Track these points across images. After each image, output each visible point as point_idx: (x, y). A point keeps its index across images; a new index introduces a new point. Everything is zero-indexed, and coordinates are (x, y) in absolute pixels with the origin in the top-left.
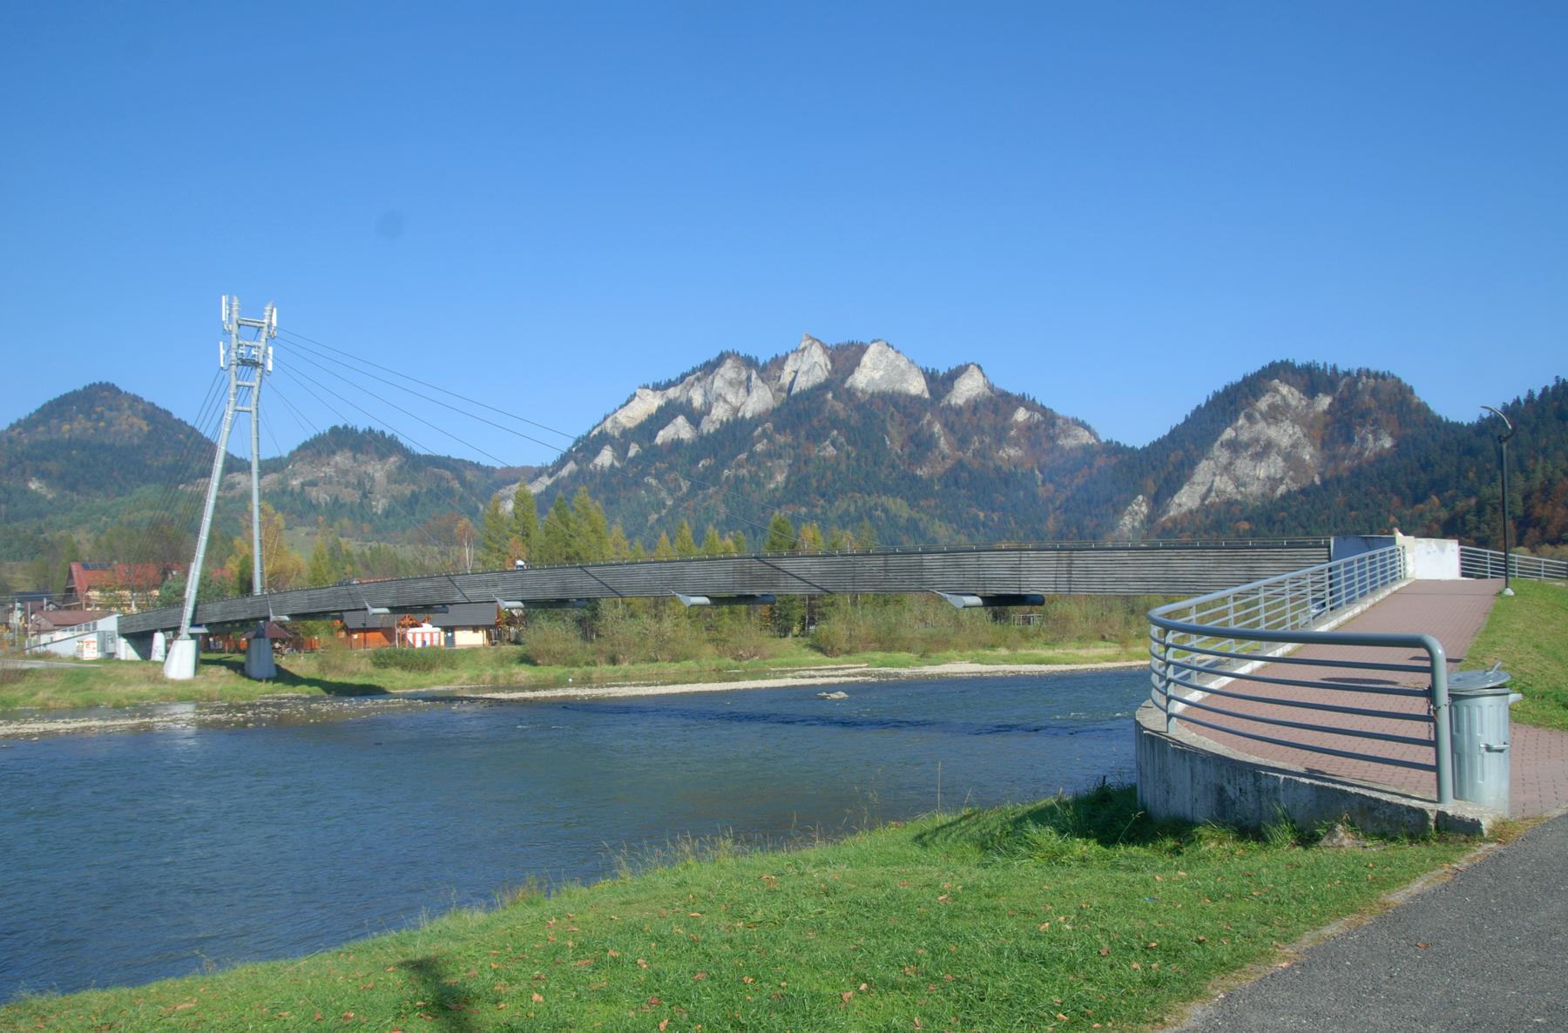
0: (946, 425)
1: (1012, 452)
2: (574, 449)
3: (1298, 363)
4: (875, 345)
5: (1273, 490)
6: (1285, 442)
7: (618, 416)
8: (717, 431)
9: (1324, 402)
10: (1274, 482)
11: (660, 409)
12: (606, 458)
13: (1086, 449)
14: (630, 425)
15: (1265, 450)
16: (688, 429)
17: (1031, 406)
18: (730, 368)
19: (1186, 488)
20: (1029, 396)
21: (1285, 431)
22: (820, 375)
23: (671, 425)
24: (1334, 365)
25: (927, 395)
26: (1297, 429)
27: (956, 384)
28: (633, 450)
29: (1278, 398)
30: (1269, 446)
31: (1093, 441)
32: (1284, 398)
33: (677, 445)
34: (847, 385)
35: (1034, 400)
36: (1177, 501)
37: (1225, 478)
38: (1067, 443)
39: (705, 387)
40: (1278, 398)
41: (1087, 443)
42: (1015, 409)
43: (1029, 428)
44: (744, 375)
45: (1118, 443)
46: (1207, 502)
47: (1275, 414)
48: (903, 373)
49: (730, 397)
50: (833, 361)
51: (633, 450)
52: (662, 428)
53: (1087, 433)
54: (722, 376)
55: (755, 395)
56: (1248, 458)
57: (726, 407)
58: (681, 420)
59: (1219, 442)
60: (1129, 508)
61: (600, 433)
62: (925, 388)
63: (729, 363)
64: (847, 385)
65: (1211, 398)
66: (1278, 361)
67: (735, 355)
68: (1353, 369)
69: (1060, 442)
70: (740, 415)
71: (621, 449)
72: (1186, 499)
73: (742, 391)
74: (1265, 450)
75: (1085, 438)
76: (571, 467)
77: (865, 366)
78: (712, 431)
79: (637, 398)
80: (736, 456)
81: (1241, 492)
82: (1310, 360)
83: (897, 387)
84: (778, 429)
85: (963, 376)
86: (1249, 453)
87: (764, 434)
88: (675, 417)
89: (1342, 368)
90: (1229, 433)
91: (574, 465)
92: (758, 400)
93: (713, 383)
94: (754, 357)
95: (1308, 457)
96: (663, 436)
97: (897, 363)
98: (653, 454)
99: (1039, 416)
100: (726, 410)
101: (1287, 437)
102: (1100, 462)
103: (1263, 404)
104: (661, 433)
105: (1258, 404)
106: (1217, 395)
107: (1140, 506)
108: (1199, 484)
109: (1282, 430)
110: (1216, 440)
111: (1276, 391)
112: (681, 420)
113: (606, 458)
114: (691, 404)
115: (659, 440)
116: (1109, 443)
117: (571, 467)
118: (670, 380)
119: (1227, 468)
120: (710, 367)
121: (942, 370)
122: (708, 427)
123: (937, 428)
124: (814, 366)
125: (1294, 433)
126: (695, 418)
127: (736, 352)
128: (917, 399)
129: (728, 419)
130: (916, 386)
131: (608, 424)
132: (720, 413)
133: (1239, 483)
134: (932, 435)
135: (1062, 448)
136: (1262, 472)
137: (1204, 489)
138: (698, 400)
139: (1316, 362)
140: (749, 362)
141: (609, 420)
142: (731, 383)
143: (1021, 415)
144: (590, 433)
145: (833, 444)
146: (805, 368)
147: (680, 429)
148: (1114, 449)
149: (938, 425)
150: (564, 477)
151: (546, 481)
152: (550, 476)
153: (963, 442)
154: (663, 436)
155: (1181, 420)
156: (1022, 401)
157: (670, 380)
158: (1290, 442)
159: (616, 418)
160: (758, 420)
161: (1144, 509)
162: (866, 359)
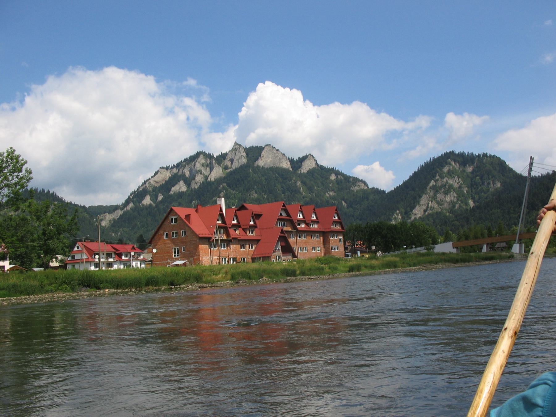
0: (304, 183)
1: (331, 193)
2: (131, 197)
3: (457, 152)
4: (267, 147)
5: (454, 207)
6: (456, 185)
7: (151, 181)
8: (199, 188)
9: (470, 169)
10: (453, 204)
11: (170, 178)
12: (147, 201)
13: (364, 191)
14: (157, 185)
15: (448, 189)
16: (185, 186)
17: (337, 173)
18: (202, 159)
19: (417, 207)
20: (335, 168)
21: (455, 181)
22: (244, 161)
23: (177, 185)
24: (472, 153)
25: (291, 169)
26: (460, 180)
27: (303, 164)
28: (160, 197)
29: (451, 167)
30: (451, 186)
31: (366, 188)
32: (453, 167)
33: (180, 194)
34: (256, 165)
35: (338, 170)
36: (414, 213)
37: (434, 202)
38: (355, 189)
39: (191, 167)
40: (451, 167)
41: (364, 189)
42: (330, 175)
43: (338, 182)
44: (208, 161)
45: (377, 188)
46: (426, 213)
47: (451, 174)
48: (280, 159)
49: (204, 171)
50: (247, 154)
51: (160, 197)
52: (173, 186)
53: (363, 184)
54: (199, 162)
55: (215, 170)
56: (442, 194)
57: (202, 176)
58: (181, 183)
59: (429, 187)
60: (394, 216)
61: (143, 189)
62: (290, 166)
63: (201, 156)
64: (256, 165)
65: (419, 168)
66: (448, 152)
67: (204, 154)
68: (480, 154)
69: (352, 189)
70: (209, 179)
71: (154, 197)
72: (418, 212)
73: (208, 169)
74: (448, 189)
75: (362, 186)
76: (131, 205)
77: (263, 157)
78: (196, 187)
79: (159, 173)
80: (213, 198)
81: (441, 208)
82: (462, 151)
83: (278, 165)
84: (229, 185)
85: (306, 160)
86: (442, 191)
87: (223, 187)
88: (179, 181)
89: (476, 153)
90: (432, 183)
91: (132, 204)
92: (217, 173)
93: (195, 165)
94: (212, 155)
95: (466, 192)
96: (175, 189)
97: (277, 155)
98: (170, 199)
99: (342, 177)
100: (202, 178)
101: (456, 184)
102: (371, 197)
103: (446, 169)
104: (173, 189)
105: (444, 170)
106: (422, 167)
107: (398, 215)
108: (422, 205)
109: (454, 181)
110: (428, 186)
111: (450, 164)
112: (181, 183)
113: (147, 201)
114: (185, 175)
115: (172, 193)
116: (373, 189)
117: (131, 205)
118: (174, 165)
119: (434, 198)
120: (193, 159)
121: (296, 158)
122: (195, 186)
123: (299, 184)
124: (241, 157)
125: (459, 182)
126: (188, 182)
127: (204, 152)
128: (289, 169)
129: (203, 182)
130: (286, 165)
131: (147, 185)
132: (199, 178)
133: (439, 203)
134: (296, 186)
135: (353, 191)
136: (448, 199)
137: (424, 207)
138: (187, 174)
139: (464, 151)
140: (209, 156)
141: (147, 183)
142: (203, 165)
143: (333, 177)
144: (138, 189)
145: (256, 192)
146: (237, 158)
147: (181, 187)
148: (377, 192)
149: (299, 183)
150: (128, 211)
151: (120, 213)
152: (122, 209)
153: (310, 189)
154: (175, 189)
155: (408, 178)
156: (332, 171)
157: (174, 165)
158: (458, 186)
159: (150, 182)
160: (219, 181)
161: (400, 217)
162: (263, 153)
